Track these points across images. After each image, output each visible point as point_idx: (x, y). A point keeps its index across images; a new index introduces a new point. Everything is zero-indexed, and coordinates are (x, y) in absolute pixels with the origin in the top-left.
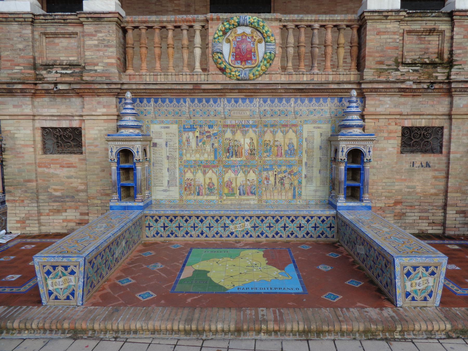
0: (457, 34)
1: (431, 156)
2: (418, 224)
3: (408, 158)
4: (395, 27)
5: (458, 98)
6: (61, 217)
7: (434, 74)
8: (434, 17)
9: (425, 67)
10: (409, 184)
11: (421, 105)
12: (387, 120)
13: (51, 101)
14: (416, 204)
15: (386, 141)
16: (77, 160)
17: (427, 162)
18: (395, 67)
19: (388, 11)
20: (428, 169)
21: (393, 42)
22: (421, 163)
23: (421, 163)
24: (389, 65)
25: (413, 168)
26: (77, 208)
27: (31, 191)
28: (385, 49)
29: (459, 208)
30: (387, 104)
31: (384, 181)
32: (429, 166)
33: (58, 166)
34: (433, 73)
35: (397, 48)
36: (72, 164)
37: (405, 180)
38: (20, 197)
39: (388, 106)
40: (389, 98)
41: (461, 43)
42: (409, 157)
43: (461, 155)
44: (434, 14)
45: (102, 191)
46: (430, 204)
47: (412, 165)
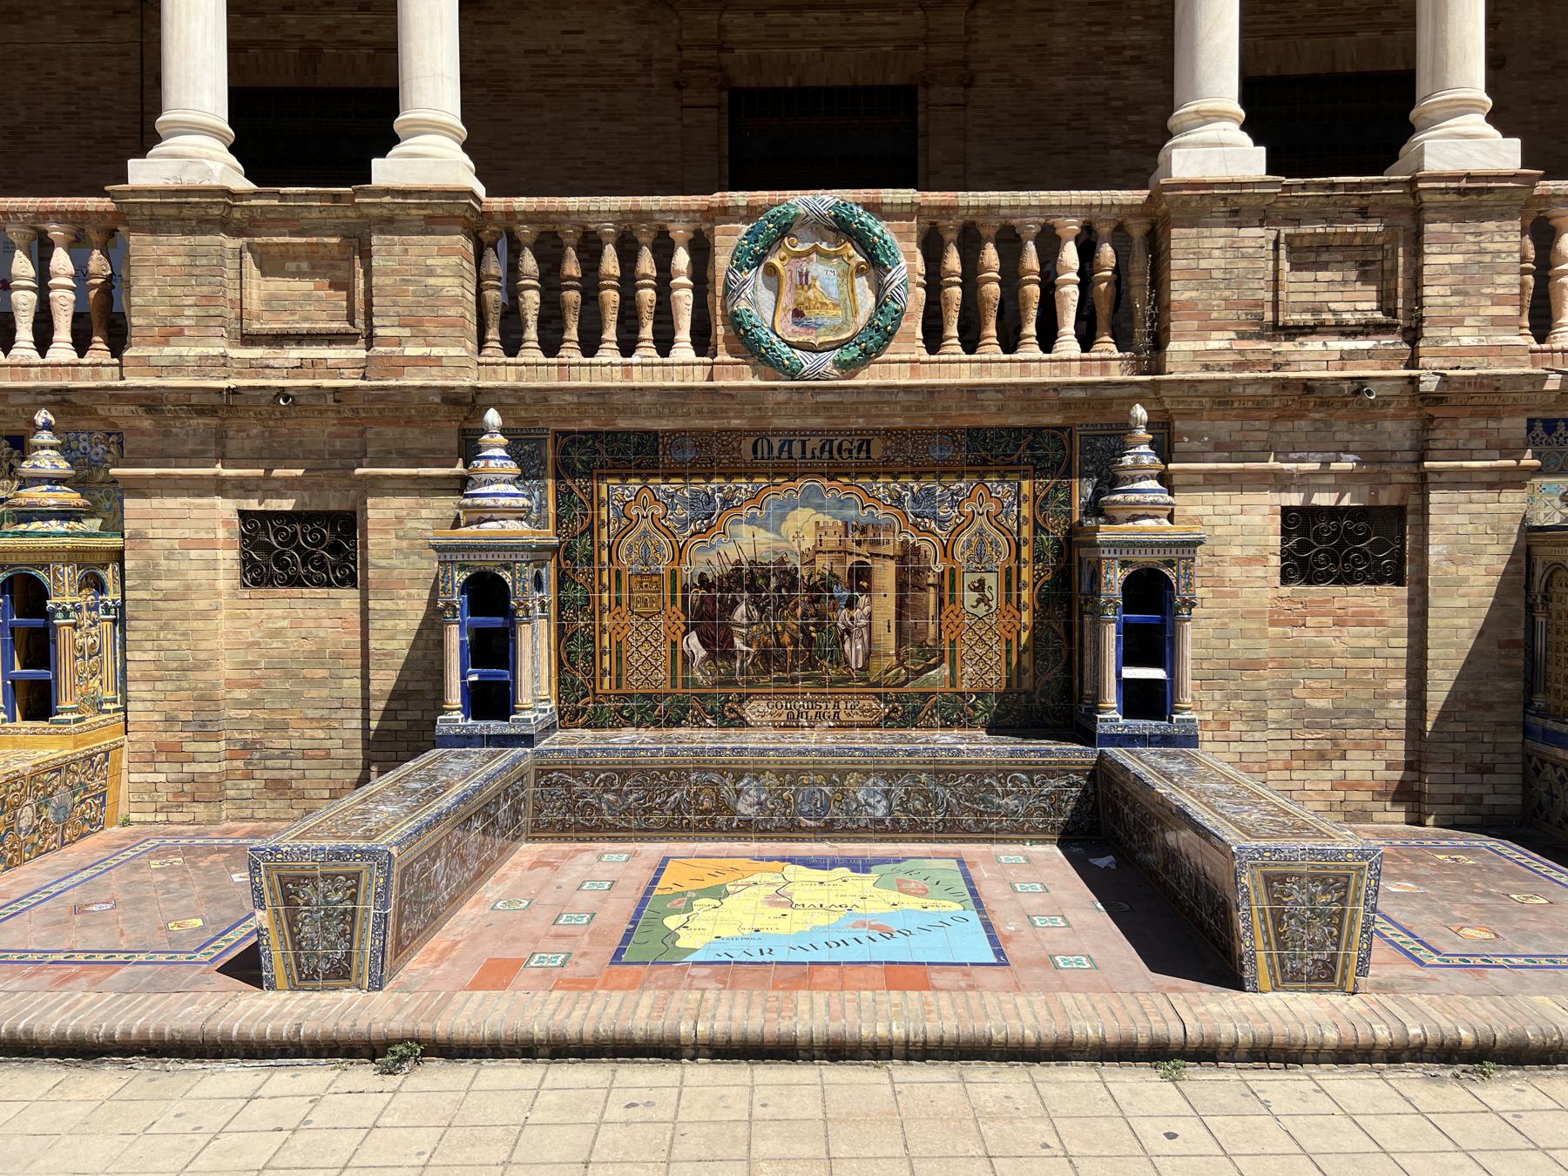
6: (1329, 775)
13: (1317, 430)
16: (1385, 602)
26: (1377, 748)
27: (1253, 695)
33: (1329, 620)
36: (1371, 614)
38: (1215, 713)
45: (1471, 696)
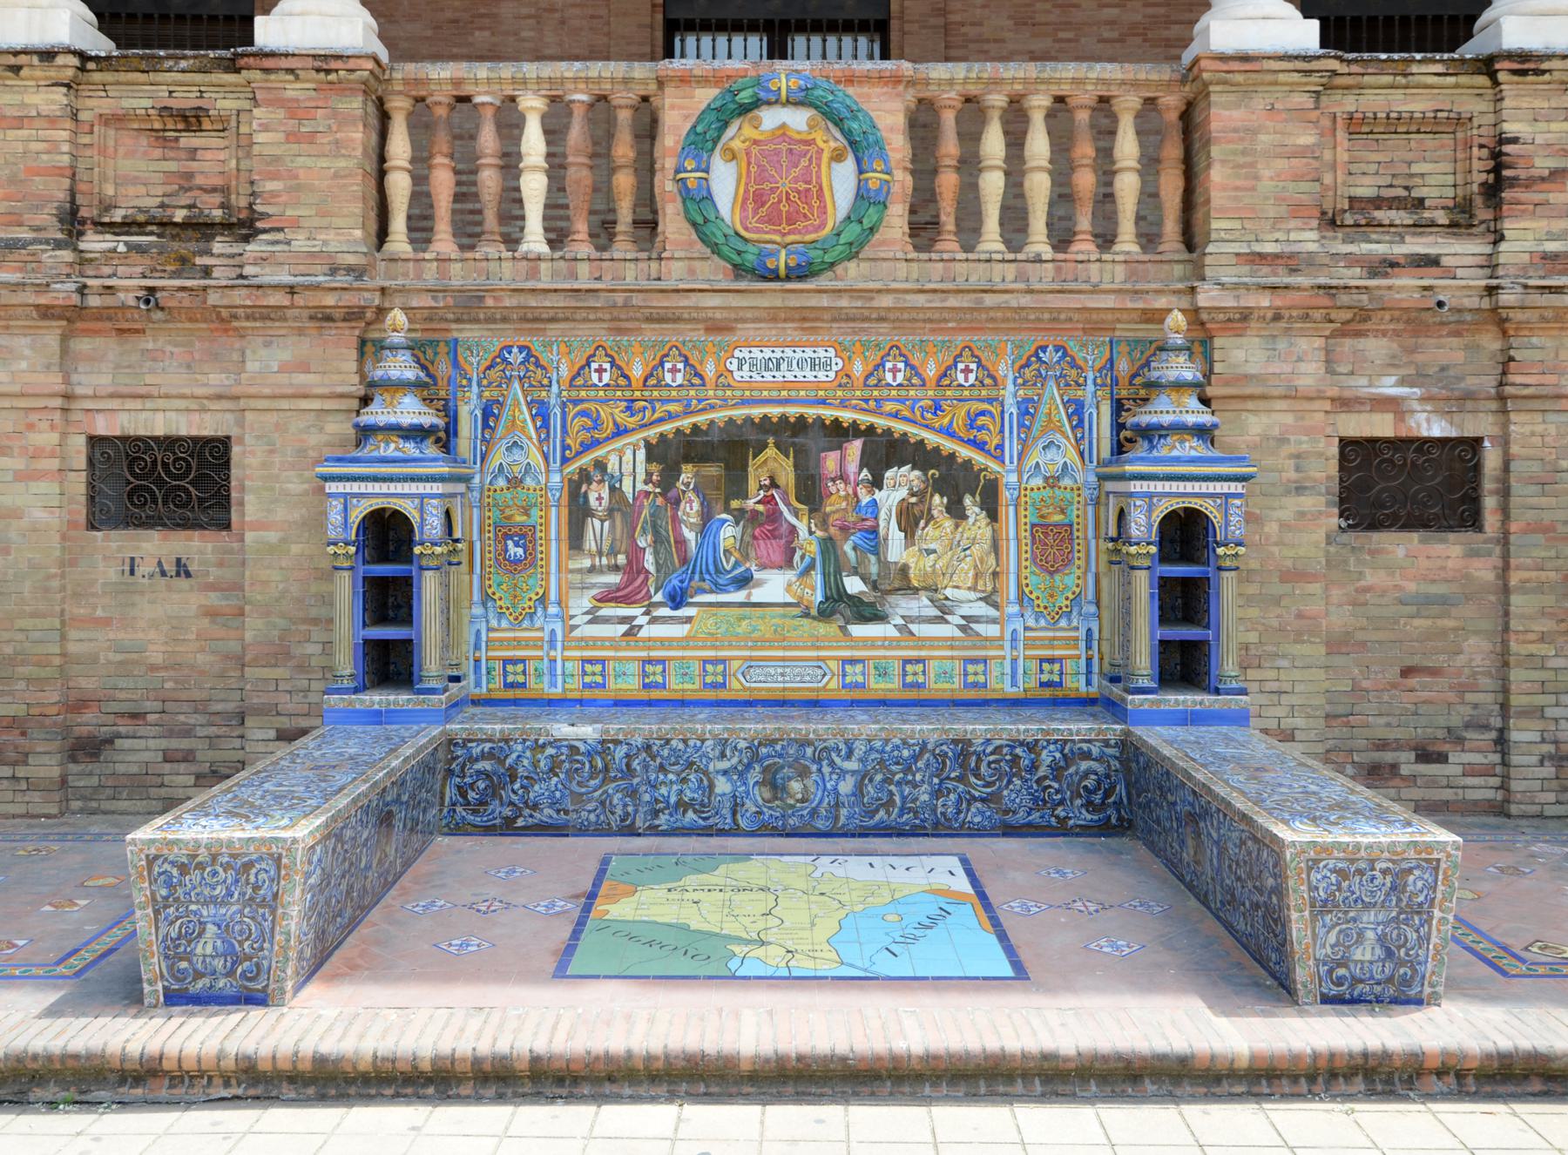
0: (265, 128)
1: (190, 539)
2: (159, 780)
3: (114, 545)
4: (53, 102)
5: (260, 339)
7: (199, 261)
8: (183, 71)
9: (173, 237)
10: (121, 635)
11: (149, 364)
12: (22, 413)
14: (149, 705)
15: (20, 486)
17: (179, 560)
18: (59, 236)
19: (16, 53)
20: (183, 583)
21: (48, 152)
22: (160, 564)
23: (160, 564)
24: (38, 229)
25: (131, 579)
28: (22, 176)
29: (285, 719)
30: (24, 358)
31: (21, 623)
32: (188, 575)
34: (194, 254)
35: (57, 171)
37: (106, 622)
39: (24, 365)
40: (29, 339)
41: (277, 159)
42: (116, 543)
43: (280, 534)
44: (183, 64)
46: (199, 707)
47: (127, 568)
